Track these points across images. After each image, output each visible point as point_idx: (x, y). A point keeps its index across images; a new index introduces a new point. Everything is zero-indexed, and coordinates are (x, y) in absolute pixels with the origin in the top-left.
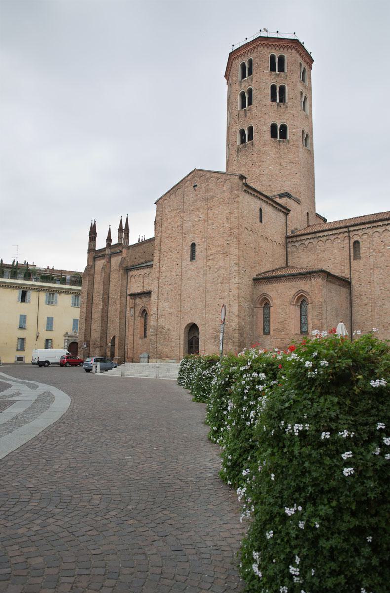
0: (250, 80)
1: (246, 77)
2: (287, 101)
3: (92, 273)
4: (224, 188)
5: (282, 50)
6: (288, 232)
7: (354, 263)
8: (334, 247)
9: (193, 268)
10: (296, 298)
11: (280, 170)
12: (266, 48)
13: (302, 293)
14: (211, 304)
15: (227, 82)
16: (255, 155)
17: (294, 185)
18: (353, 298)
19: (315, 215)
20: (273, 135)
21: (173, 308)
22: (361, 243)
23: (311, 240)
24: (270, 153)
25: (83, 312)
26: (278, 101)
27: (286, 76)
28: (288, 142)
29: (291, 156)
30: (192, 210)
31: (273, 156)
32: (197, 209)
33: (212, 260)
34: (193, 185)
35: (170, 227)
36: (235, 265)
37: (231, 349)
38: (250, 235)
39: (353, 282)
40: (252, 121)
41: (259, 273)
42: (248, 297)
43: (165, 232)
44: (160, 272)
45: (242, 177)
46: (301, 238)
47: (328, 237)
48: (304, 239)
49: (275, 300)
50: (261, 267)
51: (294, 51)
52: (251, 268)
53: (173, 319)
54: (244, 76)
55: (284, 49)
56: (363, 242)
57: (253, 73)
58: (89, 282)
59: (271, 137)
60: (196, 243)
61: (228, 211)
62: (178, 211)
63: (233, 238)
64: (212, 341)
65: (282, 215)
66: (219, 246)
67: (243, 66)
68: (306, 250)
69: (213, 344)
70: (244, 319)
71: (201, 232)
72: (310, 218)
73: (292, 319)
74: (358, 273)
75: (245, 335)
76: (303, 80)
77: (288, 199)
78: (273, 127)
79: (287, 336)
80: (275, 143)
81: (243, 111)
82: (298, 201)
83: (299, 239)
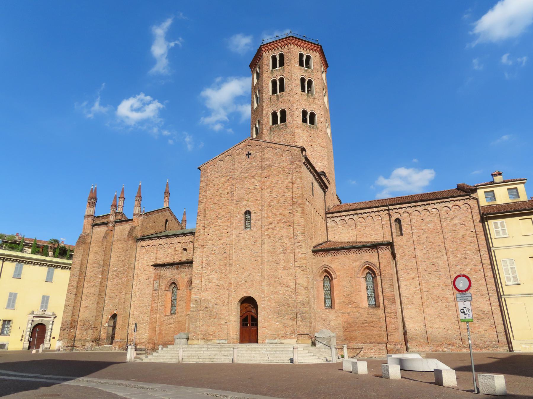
0: (281, 71)
2: (314, 94)
3: (89, 241)
4: (284, 159)
5: (308, 50)
10: (362, 270)
13: (368, 265)
14: (272, 275)
16: (289, 136)
21: (222, 279)
23: (352, 216)
28: (317, 127)
30: (246, 178)
31: (305, 138)
33: (272, 229)
34: (247, 153)
35: (218, 194)
37: (300, 325)
40: (284, 105)
44: (203, 240)
46: (342, 214)
48: (345, 215)
49: (338, 272)
53: (222, 292)
54: (274, 66)
56: (403, 219)
57: (285, 65)
58: (84, 251)
60: (251, 211)
61: (290, 180)
62: (228, 178)
64: (275, 317)
65: (322, 191)
67: (274, 58)
68: (346, 226)
69: (276, 320)
71: (257, 200)
74: (402, 249)
78: (304, 113)
79: (355, 310)
80: (307, 127)
81: (276, 96)
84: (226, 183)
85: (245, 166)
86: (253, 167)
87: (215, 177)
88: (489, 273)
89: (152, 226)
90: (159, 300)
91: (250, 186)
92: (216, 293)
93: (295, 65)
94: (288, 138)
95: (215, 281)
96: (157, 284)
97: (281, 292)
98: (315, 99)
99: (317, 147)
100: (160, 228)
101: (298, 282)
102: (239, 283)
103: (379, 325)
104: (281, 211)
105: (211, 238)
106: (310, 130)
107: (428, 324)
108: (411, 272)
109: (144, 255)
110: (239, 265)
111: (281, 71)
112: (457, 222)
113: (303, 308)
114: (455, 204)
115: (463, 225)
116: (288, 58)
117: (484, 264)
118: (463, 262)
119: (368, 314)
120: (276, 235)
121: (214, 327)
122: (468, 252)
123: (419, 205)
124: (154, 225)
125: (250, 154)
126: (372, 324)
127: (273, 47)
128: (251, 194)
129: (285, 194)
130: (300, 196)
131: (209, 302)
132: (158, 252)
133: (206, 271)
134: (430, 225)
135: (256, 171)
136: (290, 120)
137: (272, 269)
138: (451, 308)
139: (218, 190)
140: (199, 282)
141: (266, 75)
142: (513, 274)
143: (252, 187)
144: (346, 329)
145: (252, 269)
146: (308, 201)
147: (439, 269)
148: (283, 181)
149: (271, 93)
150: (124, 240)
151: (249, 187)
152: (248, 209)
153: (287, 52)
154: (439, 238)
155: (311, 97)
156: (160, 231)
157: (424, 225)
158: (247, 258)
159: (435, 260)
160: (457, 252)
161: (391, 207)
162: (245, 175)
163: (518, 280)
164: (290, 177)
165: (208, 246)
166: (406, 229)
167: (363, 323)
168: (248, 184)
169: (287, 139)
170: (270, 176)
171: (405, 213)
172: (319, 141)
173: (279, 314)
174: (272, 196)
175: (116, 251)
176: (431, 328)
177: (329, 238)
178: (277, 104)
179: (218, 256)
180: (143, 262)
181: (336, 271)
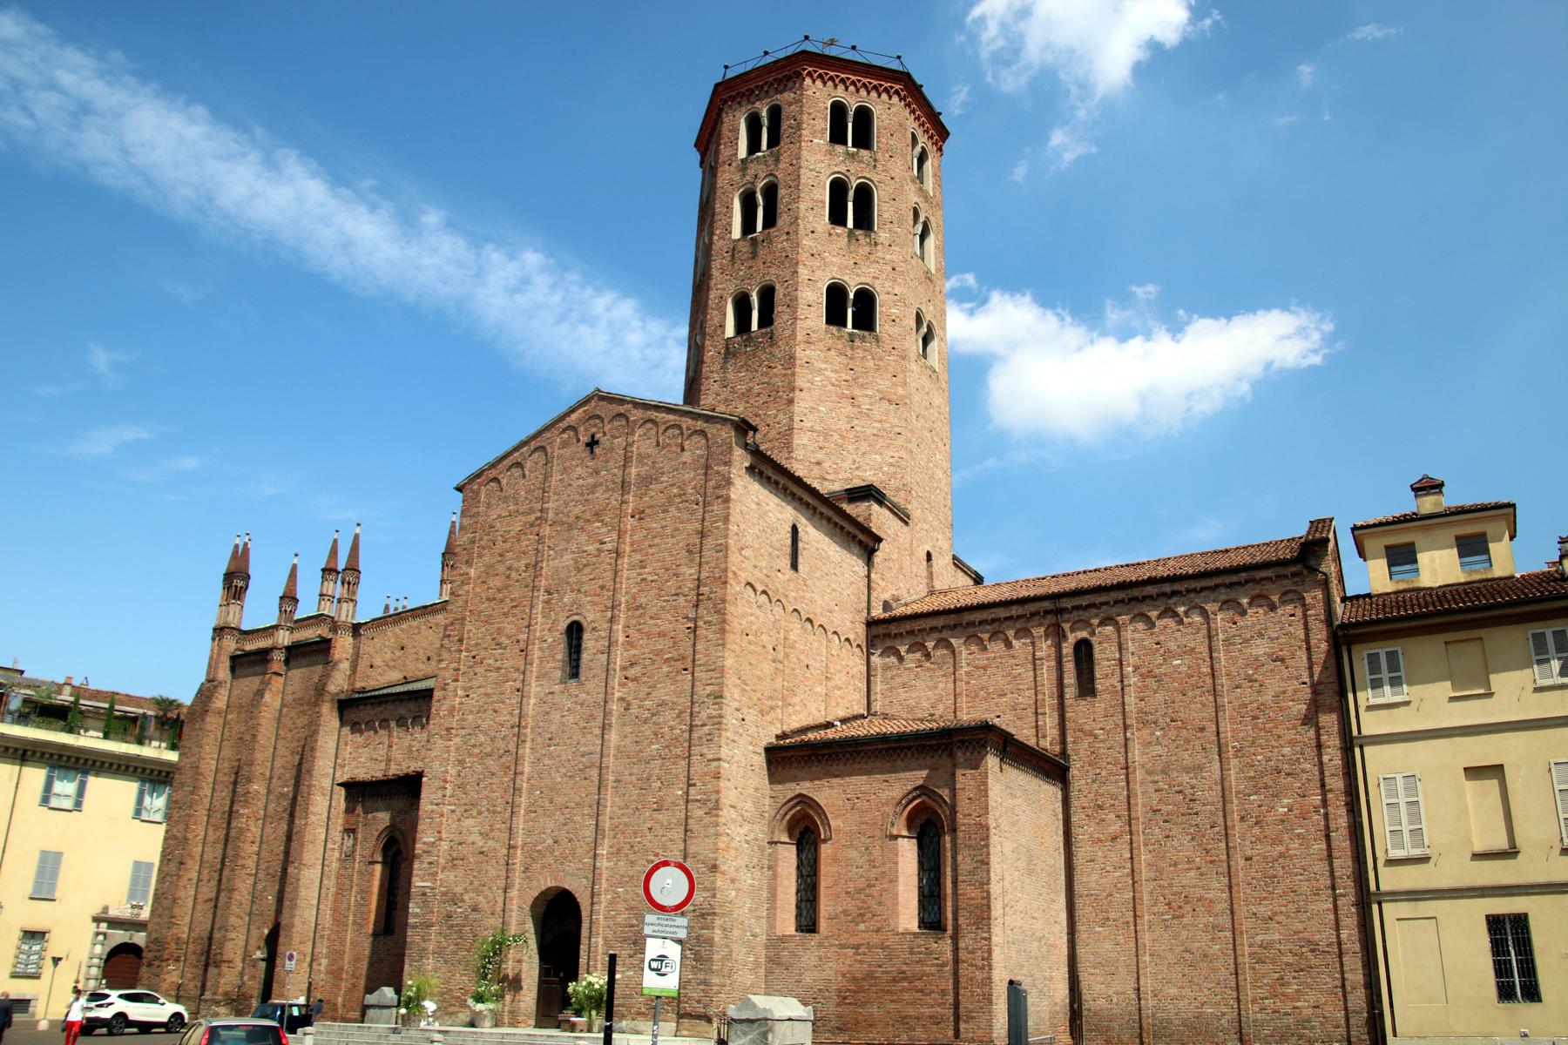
0: (771, 161)
1: (759, 151)
2: (876, 229)
4: (686, 457)
5: (863, 92)
6: (873, 604)
7: (1079, 710)
9: (569, 704)
10: (906, 813)
11: (850, 419)
12: (819, 83)
14: (626, 825)
15: (702, 163)
17: (892, 465)
19: (949, 558)
20: (835, 316)
21: (496, 834)
22: (1097, 649)
24: (823, 366)
25: (175, 837)
26: (850, 224)
27: (875, 160)
29: (884, 383)
32: (596, 514)
33: (635, 679)
35: (501, 568)
36: (710, 701)
38: (760, 607)
39: (1074, 772)
40: (772, 271)
41: (786, 728)
42: (749, 805)
43: (484, 582)
45: (744, 427)
46: (916, 625)
47: (996, 625)
49: (836, 818)
50: (790, 709)
51: (895, 99)
52: (762, 712)
53: (492, 873)
55: (869, 93)
59: (827, 323)
60: (585, 624)
62: (532, 518)
63: (709, 612)
66: (662, 635)
70: (733, 881)
71: (602, 587)
73: (890, 882)
75: (736, 933)
77: (875, 507)
78: (836, 294)
79: (875, 939)
82: (903, 516)
83: (908, 627)
84: (525, 534)
85: (581, 482)
86: (601, 484)
87: (499, 516)
88: (1341, 821)
89: (394, 660)
92: (476, 874)
93: (815, 141)
94: (776, 376)
95: (475, 838)
96: (351, 842)
98: (876, 244)
99: (871, 404)
101: (692, 849)
102: (539, 848)
103: (940, 988)
104: (665, 626)
106: (852, 349)
107: (1147, 984)
108: (1112, 816)
109: (361, 751)
110: (541, 792)
111: (770, 163)
112: (1261, 651)
113: (702, 928)
114: (1257, 591)
115: (1279, 663)
116: (792, 122)
117: (1330, 790)
119: (911, 953)
120: (645, 700)
121: (465, 975)
122: (1286, 750)
123: (1151, 597)
124: (400, 657)
126: (919, 984)
127: (752, 87)
128: (586, 571)
129: (683, 569)
130: (720, 577)
131: (454, 900)
132: (395, 740)
133: (453, 808)
134: (1179, 662)
135: (607, 496)
136: (786, 317)
137: (626, 807)
139: (501, 555)
140: (433, 840)
141: (727, 176)
142: (1411, 823)
143: (591, 548)
144: (845, 998)
145: (573, 805)
146: (760, 588)
147: (1197, 807)
148: (677, 529)
151: (586, 548)
152: (576, 618)
153: (791, 100)
154: (1204, 705)
156: (420, 675)
157: (1161, 662)
158: (564, 770)
159: (1185, 778)
160: (1252, 750)
161: (1067, 603)
162: (577, 510)
163: (1426, 843)
164: (699, 514)
165: (463, 732)
166: (1107, 675)
167: (894, 980)
168: (583, 538)
169: (774, 380)
170: (643, 512)
171: (1107, 622)
174: (645, 576)
175: (289, 736)
176: (1155, 996)
178: (751, 267)
179: (490, 762)
181: (829, 816)
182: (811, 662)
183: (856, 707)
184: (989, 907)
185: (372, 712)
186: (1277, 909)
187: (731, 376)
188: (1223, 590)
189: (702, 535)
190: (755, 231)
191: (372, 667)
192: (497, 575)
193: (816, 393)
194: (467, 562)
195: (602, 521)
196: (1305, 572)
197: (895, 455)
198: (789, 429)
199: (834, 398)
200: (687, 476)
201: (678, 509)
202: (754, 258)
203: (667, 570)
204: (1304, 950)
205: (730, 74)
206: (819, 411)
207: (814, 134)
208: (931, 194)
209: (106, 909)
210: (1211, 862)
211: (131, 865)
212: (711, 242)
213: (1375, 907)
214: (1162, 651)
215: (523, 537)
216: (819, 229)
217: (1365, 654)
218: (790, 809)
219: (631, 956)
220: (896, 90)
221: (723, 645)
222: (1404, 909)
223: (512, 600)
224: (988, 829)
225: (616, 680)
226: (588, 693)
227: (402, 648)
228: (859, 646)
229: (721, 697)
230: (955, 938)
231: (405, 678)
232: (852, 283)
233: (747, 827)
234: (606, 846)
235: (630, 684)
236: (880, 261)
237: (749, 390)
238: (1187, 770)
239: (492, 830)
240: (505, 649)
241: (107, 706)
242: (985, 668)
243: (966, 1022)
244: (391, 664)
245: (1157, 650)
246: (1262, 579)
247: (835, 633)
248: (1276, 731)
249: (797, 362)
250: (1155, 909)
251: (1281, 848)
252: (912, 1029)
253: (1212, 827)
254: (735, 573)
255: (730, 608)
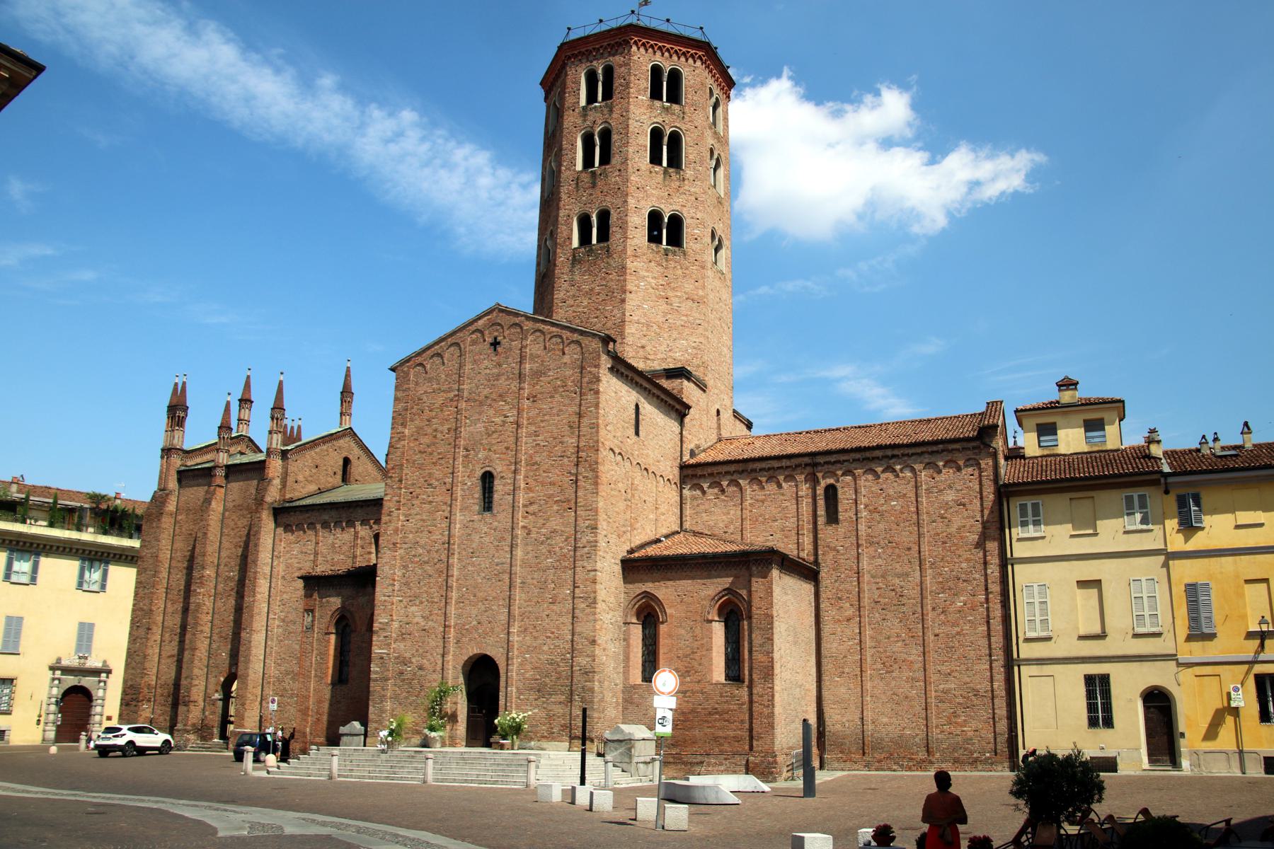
0: (606, 111)
1: (596, 102)
4: (566, 359)
5: (675, 58)
6: (684, 453)
7: (826, 533)
8: (783, 495)
9: (485, 529)
10: (717, 606)
11: (665, 314)
12: (642, 50)
15: (546, 99)
16: (614, 276)
18: (822, 606)
19: (731, 412)
21: (434, 617)
22: (840, 492)
24: (646, 274)
26: (665, 163)
27: (683, 113)
29: (689, 286)
33: (534, 514)
35: (429, 431)
36: (589, 531)
39: (823, 574)
40: (608, 199)
41: (633, 545)
42: (612, 599)
45: (607, 340)
46: (715, 470)
47: (771, 472)
49: (671, 607)
50: (635, 532)
51: (699, 63)
55: (679, 58)
60: (495, 474)
62: (452, 395)
63: (586, 470)
70: (604, 650)
71: (507, 448)
72: (722, 421)
74: (832, 554)
75: (606, 683)
76: (714, 123)
77: (686, 382)
78: (655, 218)
79: (697, 687)
80: (658, 252)
81: (589, 175)
82: (702, 387)
83: (709, 471)
84: (446, 406)
85: (488, 371)
86: (503, 374)
88: (997, 612)
89: (311, 476)
90: (315, 652)
91: (495, 418)
92: (420, 644)
93: (640, 97)
96: (310, 619)
97: (545, 648)
98: (684, 180)
99: (680, 303)
100: (330, 479)
101: (578, 629)
102: (466, 627)
104: (554, 478)
105: (414, 528)
106: (667, 261)
107: (869, 715)
108: (848, 605)
111: (605, 112)
113: (586, 681)
115: (962, 507)
116: (622, 81)
117: (991, 592)
118: (952, 586)
119: (721, 696)
121: (415, 713)
122: (964, 565)
123: (878, 458)
124: (315, 474)
125: (499, 343)
126: (726, 716)
127: (591, 48)
128: (495, 436)
129: (566, 439)
131: (405, 662)
132: (321, 539)
133: (400, 598)
135: (508, 383)
136: (618, 236)
137: (530, 600)
138: (918, 684)
139: (429, 421)
141: (572, 119)
142: (1041, 615)
143: (498, 420)
144: (677, 725)
145: (491, 598)
146: (617, 451)
147: (904, 600)
148: (562, 410)
149: (579, 166)
150: (248, 508)
152: (488, 469)
153: (621, 63)
155: (674, 176)
156: (329, 486)
158: (484, 575)
159: (897, 581)
160: (941, 564)
161: (821, 460)
162: (486, 391)
163: (1050, 629)
165: (406, 546)
166: (846, 510)
167: (710, 714)
168: (491, 412)
170: (535, 396)
172: (686, 286)
173: (540, 690)
175: (232, 533)
176: (874, 723)
177: (684, 524)
178: (591, 195)
179: (427, 567)
180: (289, 561)
182: (646, 498)
183: (673, 527)
184: (773, 667)
185: (301, 517)
186: (954, 668)
187: (577, 278)
188: (927, 456)
189: (580, 415)
190: (593, 166)
191: (296, 482)
192: (426, 435)
193: (641, 294)
194: (402, 424)
195: (505, 401)
196: (982, 447)
197: (697, 340)
198: (622, 322)
199: (654, 298)
200: (567, 373)
201: (562, 396)
202: (593, 187)
203: (555, 438)
204: (970, 695)
205: (574, 36)
206: (644, 308)
207: (639, 91)
208: (722, 134)
209: (59, 660)
210: (912, 637)
211: (77, 626)
212: (560, 171)
213: (1016, 669)
214: (884, 495)
215: (445, 409)
216: (643, 168)
217: (1018, 504)
218: (638, 601)
219: (536, 700)
220: (700, 56)
221: (597, 493)
222: (1034, 670)
223: (439, 454)
224: (772, 618)
225: (520, 514)
226: (499, 522)
227: (317, 467)
228: (675, 483)
229: (596, 528)
230: (750, 687)
231: (319, 489)
232: (666, 210)
233: (611, 613)
234: (516, 627)
235: (530, 517)
236: (687, 193)
237: (592, 290)
238: (898, 576)
239: (431, 615)
240: (435, 488)
241: (51, 501)
242: (763, 501)
243: (757, 740)
244: (310, 479)
245: (881, 494)
246: (953, 450)
247: (661, 476)
248: (957, 552)
249: (628, 271)
250: (875, 667)
251: (958, 629)
252: (721, 745)
253: (913, 614)
254: (603, 443)
255: (601, 468)
